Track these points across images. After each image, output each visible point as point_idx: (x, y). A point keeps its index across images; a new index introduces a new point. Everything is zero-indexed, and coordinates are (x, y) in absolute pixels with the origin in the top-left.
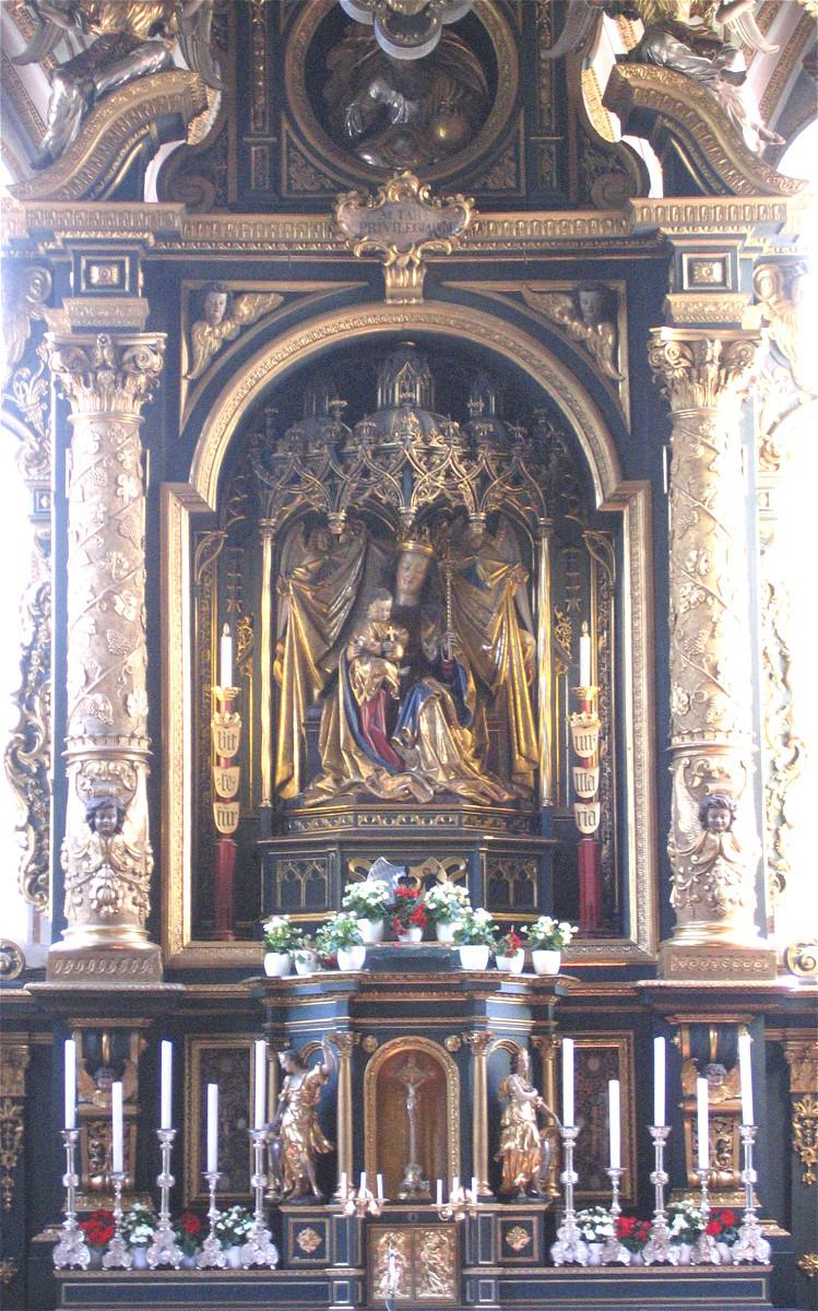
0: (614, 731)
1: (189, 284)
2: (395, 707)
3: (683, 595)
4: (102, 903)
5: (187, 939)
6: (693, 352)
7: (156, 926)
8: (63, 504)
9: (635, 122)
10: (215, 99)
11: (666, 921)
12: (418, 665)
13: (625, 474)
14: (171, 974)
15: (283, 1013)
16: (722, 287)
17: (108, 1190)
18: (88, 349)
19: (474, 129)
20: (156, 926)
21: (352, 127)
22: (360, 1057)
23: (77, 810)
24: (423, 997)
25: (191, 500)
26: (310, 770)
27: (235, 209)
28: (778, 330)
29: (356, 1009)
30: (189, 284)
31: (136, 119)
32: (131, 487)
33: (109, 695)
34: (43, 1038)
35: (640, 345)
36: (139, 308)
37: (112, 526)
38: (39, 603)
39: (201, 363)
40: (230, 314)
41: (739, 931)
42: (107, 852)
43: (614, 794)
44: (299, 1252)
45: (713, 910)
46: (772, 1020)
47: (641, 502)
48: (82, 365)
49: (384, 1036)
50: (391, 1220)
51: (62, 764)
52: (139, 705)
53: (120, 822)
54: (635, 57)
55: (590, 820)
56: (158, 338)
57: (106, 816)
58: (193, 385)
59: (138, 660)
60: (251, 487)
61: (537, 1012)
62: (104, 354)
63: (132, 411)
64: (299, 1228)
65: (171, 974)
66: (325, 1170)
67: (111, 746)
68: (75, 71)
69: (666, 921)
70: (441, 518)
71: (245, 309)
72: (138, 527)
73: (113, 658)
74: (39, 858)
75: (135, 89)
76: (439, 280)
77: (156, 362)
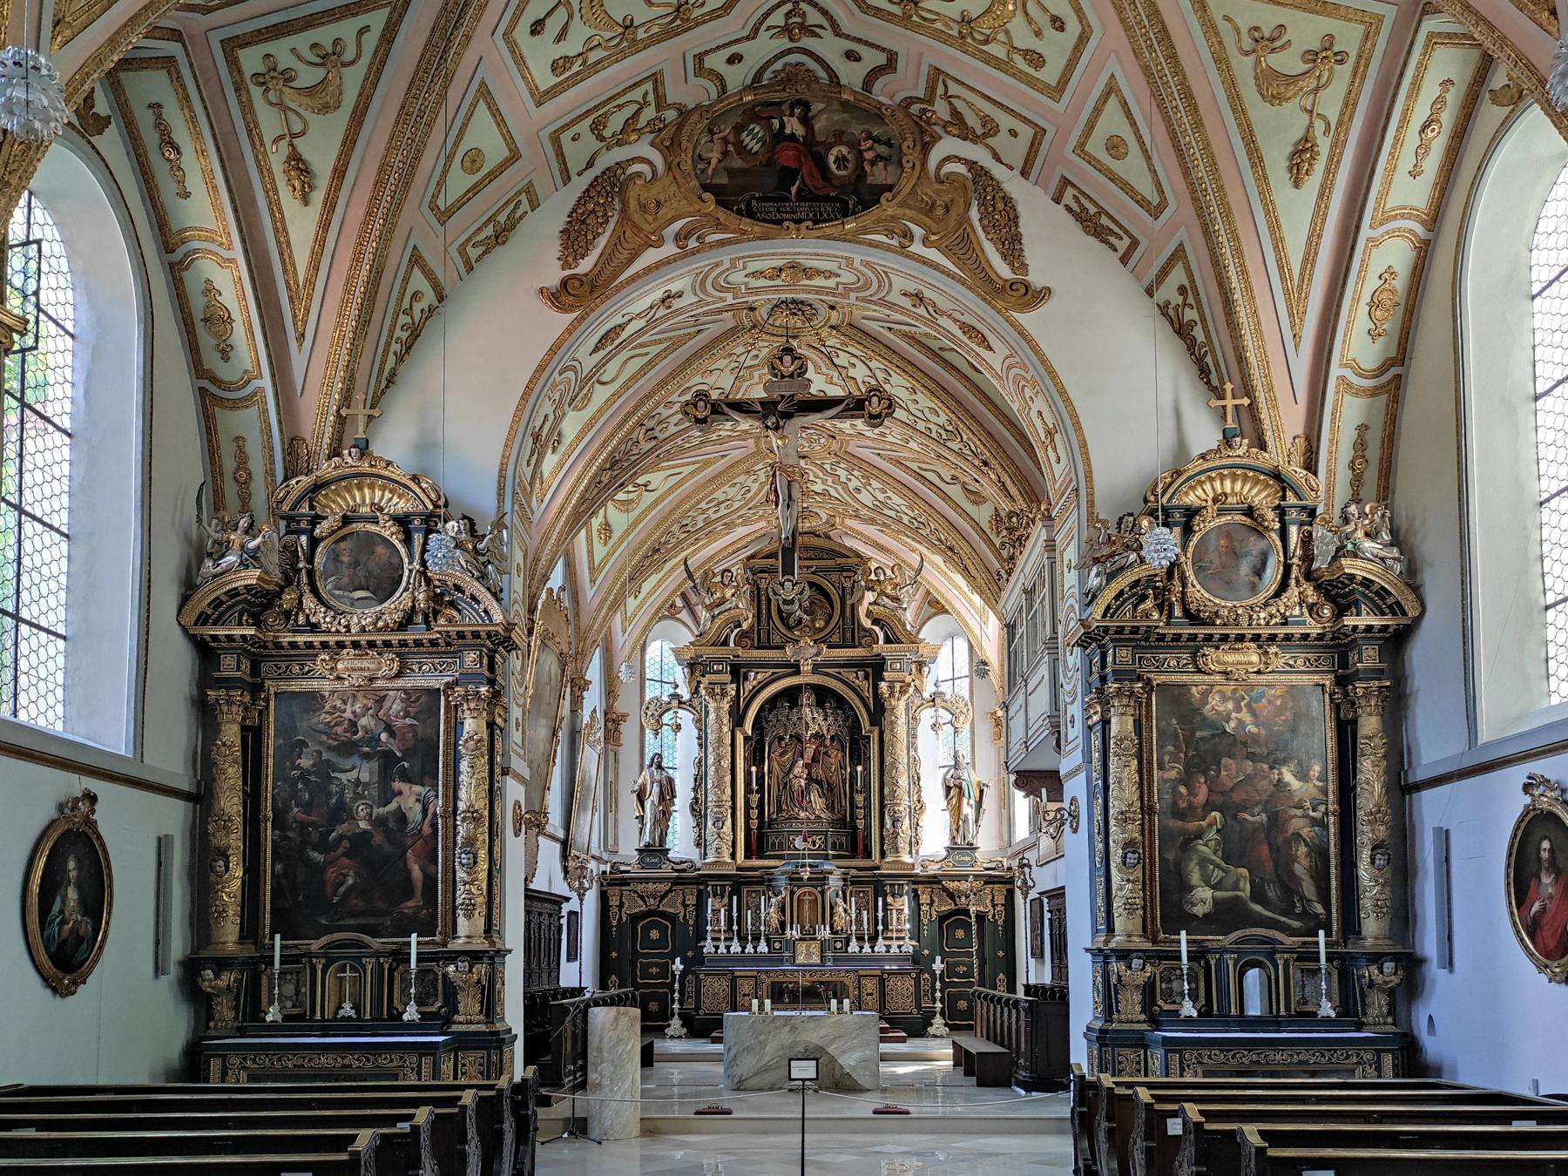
0: (868, 799)
2: (804, 793)
3: (888, 760)
6: (891, 688)
7: (733, 855)
8: (706, 734)
9: (876, 622)
10: (750, 616)
11: (883, 854)
12: (810, 779)
13: (872, 725)
14: (738, 869)
15: (770, 880)
16: (901, 670)
17: (720, 931)
19: (827, 623)
20: (733, 855)
21: (791, 622)
23: (710, 823)
25: (744, 733)
26: (780, 810)
27: (757, 648)
28: (917, 683)
31: (727, 622)
32: (726, 729)
34: (701, 887)
35: (876, 688)
36: (728, 677)
37: (720, 741)
38: (700, 762)
41: (907, 859)
42: (719, 835)
43: (868, 816)
45: (897, 850)
46: (914, 883)
47: (876, 733)
48: (712, 694)
50: (801, 939)
51: (706, 808)
52: (728, 791)
54: (875, 603)
55: (861, 824)
56: (734, 686)
57: (719, 821)
59: (728, 779)
60: (762, 728)
61: (845, 880)
62: (718, 690)
63: (726, 706)
65: (738, 869)
68: (709, 608)
69: (883, 854)
70: (817, 736)
72: (728, 741)
73: (720, 778)
74: (700, 836)
76: (816, 669)
77: (733, 693)
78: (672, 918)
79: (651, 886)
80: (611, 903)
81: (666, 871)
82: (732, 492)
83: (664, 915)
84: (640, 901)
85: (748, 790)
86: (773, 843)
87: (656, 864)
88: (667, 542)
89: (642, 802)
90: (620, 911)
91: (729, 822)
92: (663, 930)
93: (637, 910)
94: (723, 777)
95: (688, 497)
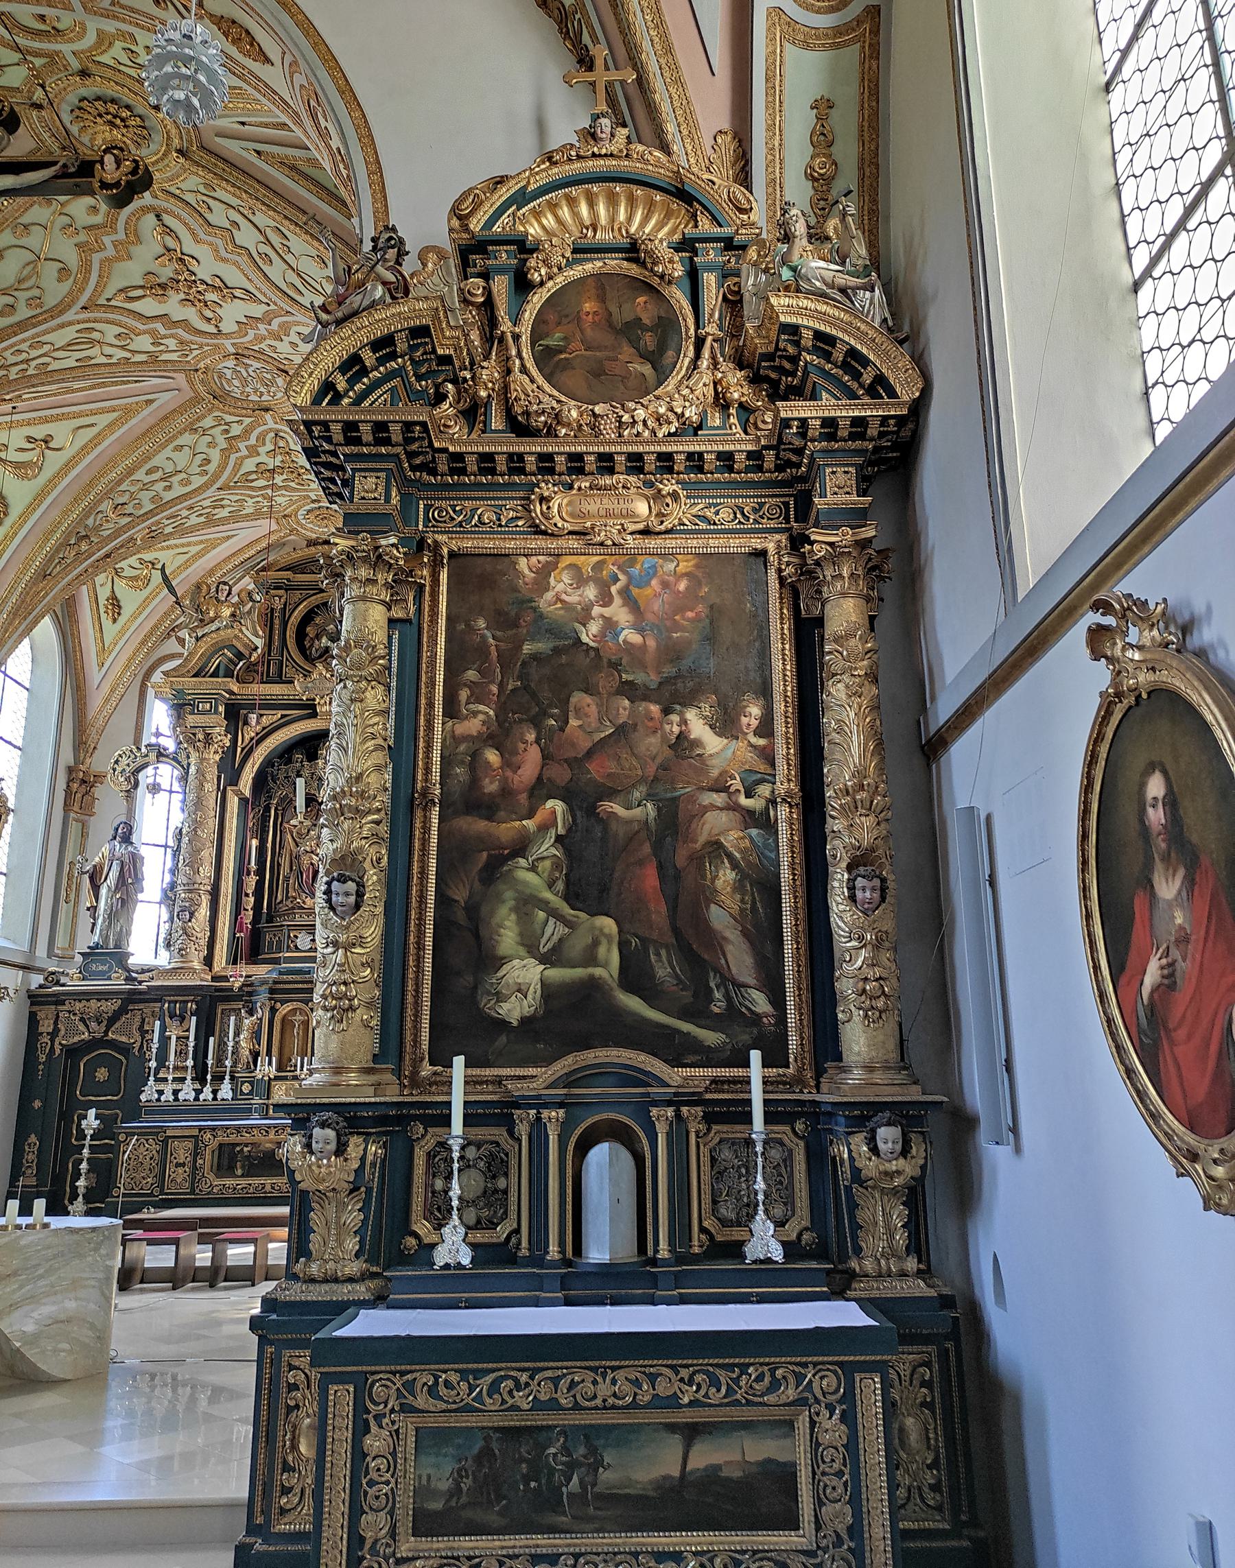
1: (243, 712)
4: (180, 950)
5: (223, 965)
7: (208, 961)
18: (194, 735)
20: (208, 961)
22: (273, 1011)
24: (300, 986)
25: (239, 793)
29: (272, 991)
30: (243, 712)
32: (210, 787)
33: (192, 867)
39: (246, 741)
40: (258, 723)
42: (184, 929)
44: (242, 1093)
49: (283, 1002)
52: (207, 871)
53: (191, 918)
58: (243, 749)
62: (201, 736)
64: (243, 1083)
65: (214, 979)
66: (255, 1055)
67: (191, 887)
71: (265, 721)
72: (211, 802)
75: (213, 635)
78: (125, 1049)
79: (94, 1004)
80: (41, 1029)
81: (117, 982)
82: (182, 459)
83: (113, 1044)
84: (82, 1027)
85: (241, 871)
86: (271, 943)
87: (102, 973)
88: (97, 528)
89: (96, 888)
90: (52, 1041)
91: (203, 912)
92: (113, 1066)
93: (76, 1039)
94: (199, 851)
95: (113, 462)
